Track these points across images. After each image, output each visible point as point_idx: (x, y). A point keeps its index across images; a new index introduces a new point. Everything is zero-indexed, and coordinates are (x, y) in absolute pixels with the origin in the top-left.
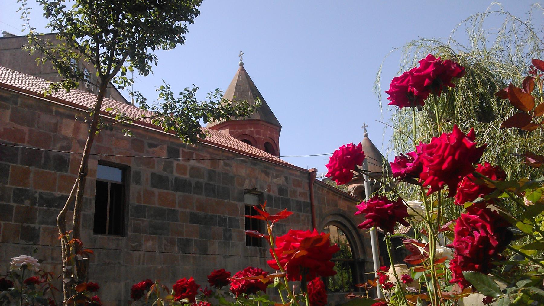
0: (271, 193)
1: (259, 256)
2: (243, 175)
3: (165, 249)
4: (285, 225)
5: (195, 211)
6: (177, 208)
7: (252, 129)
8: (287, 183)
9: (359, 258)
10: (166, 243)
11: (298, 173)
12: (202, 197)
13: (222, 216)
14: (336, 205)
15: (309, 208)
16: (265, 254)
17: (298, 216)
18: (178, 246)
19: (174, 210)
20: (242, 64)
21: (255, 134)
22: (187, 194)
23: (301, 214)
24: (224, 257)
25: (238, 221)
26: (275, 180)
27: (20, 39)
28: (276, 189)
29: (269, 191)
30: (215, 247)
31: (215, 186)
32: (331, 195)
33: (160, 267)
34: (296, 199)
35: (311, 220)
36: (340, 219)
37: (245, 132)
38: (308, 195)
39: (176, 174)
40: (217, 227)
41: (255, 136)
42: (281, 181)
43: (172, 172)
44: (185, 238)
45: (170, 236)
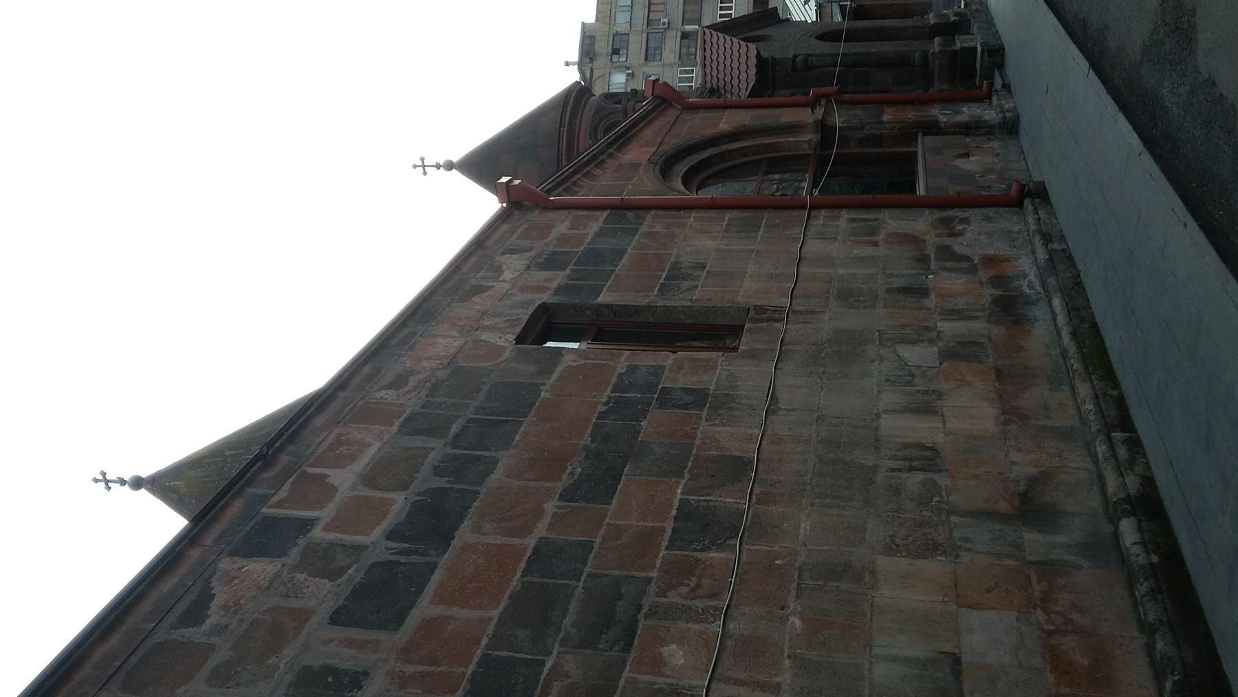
0: (554, 285)
3: (713, 596)
5: (559, 487)
6: (531, 542)
8: (529, 250)
9: (809, 142)
10: (685, 590)
11: (505, 228)
12: (506, 459)
13: (601, 408)
15: (630, 215)
18: (706, 549)
19: (536, 550)
22: (476, 504)
24: (775, 413)
25: (632, 369)
28: (540, 276)
31: (471, 420)
32: (597, 172)
33: (797, 622)
35: (674, 212)
36: (682, 168)
44: (669, 526)
45: (654, 574)
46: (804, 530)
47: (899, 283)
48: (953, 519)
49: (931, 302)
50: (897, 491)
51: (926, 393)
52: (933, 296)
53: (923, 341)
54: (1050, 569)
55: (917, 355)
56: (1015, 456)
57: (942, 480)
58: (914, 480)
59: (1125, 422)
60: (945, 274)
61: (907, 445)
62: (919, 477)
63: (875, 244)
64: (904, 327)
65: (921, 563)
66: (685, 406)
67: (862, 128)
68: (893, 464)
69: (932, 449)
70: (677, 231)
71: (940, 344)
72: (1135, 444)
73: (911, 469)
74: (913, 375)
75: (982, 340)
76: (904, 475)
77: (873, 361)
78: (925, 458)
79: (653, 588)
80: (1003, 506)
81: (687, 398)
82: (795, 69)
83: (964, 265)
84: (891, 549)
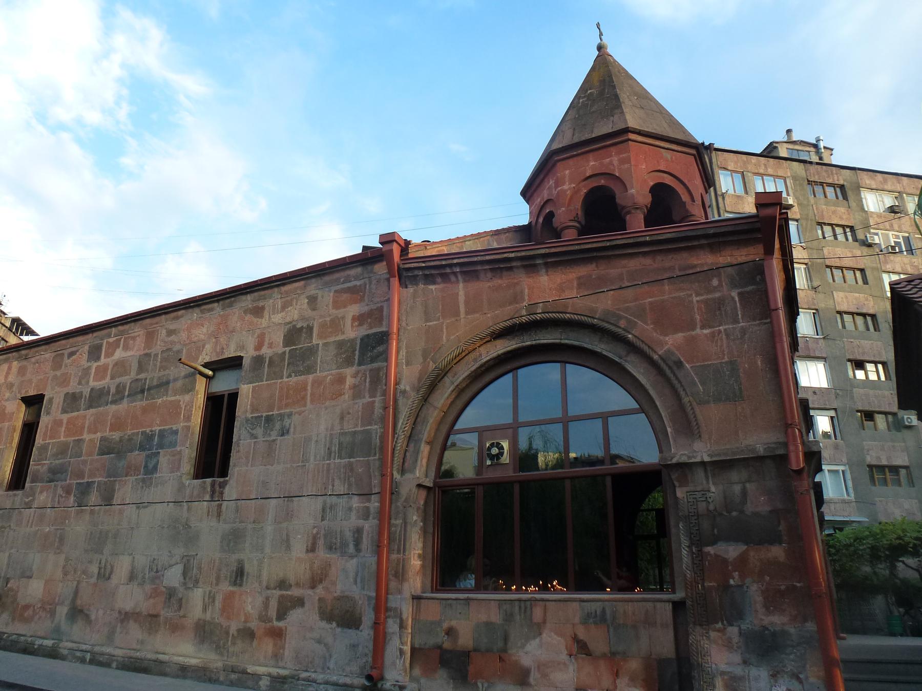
1: (207, 497)
2: (202, 337)
4: (290, 415)
5: (107, 434)
13: (148, 430)
14: (516, 299)
16: (222, 493)
18: (75, 496)
20: (600, 48)
24: (138, 508)
26: (278, 318)
29: (258, 347)
30: (126, 490)
34: (340, 337)
39: (92, 383)
40: (137, 452)
43: (88, 382)
44: (86, 480)
46: (78, 528)
47: (247, 568)
48: (75, 583)
49: (226, 587)
50: (90, 562)
51: (144, 577)
52: (231, 588)
53: (185, 578)
54: (53, 613)
55: (173, 577)
56: (101, 612)
57: (93, 580)
58: (94, 569)
59: (93, 662)
60: (259, 600)
61: (112, 567)
62: (96, 571)
63: (312, 549)
64: (200, 569)
65: (60, 569)
66: (146, 466)
68: (103, 562)
69: (109, 578)
71: (181, 589)
72: (82, 661)
73: (100, 568)
74: (157, 572)
75: (182, 613)
76: (97, 565)
77: (170, 552)
78: (105, 575)
79: (63, 483)
80: (79, 602)
81: (151, 466)
83: (272, 613)
84: (67, 560)
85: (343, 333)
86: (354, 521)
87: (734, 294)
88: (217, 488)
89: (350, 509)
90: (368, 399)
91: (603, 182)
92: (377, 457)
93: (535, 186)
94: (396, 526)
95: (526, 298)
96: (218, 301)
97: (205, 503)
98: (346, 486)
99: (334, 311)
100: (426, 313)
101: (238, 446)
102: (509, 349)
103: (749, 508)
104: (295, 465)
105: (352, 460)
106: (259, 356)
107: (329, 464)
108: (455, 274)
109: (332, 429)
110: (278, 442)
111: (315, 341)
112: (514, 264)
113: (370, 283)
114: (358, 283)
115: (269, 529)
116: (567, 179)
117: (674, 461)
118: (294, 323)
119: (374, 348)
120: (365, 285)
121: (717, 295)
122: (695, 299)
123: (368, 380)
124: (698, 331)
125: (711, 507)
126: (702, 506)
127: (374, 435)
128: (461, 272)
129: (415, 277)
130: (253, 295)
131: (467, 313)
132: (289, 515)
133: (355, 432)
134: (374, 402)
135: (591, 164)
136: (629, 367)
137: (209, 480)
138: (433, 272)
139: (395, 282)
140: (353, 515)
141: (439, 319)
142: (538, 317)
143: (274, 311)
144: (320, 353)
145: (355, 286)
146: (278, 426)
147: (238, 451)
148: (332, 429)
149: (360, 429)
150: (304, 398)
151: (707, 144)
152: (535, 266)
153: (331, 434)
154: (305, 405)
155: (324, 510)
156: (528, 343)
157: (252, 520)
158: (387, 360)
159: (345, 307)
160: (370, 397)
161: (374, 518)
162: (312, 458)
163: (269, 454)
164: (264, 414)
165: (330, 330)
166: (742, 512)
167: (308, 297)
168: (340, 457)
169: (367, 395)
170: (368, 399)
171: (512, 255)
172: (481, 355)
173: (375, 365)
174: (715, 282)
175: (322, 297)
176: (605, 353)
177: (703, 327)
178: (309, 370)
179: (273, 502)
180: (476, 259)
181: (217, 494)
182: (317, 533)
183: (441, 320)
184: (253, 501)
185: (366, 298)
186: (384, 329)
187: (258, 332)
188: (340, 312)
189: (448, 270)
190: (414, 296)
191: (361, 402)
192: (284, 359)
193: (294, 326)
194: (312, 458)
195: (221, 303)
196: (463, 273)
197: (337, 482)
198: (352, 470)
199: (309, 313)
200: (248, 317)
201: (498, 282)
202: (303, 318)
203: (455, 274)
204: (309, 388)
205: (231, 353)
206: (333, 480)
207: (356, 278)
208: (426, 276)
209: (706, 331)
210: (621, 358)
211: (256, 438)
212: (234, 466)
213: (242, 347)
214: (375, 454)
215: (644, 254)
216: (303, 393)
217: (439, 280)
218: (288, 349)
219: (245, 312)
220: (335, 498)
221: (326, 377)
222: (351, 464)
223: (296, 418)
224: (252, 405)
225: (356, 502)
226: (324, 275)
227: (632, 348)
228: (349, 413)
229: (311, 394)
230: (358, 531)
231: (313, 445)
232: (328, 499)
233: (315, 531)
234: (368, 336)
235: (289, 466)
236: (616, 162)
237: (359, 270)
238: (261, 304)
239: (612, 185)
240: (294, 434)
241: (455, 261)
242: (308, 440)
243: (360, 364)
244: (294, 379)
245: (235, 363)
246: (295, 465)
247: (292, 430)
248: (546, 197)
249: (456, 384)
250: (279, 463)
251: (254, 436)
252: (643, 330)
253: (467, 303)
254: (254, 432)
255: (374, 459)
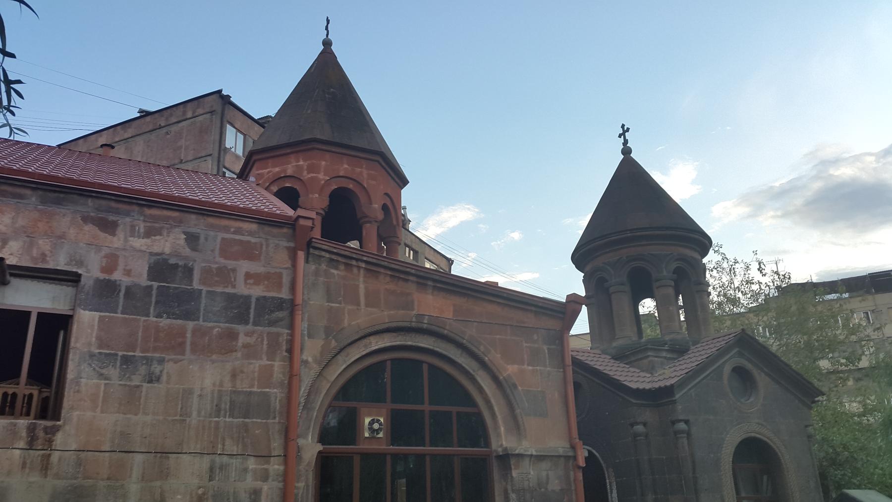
4: (161, 361)
7: (301, 163)
14: (409, 306)
16: (50, 441)
17: (232, 336)
20: (327, 43)
21: (305, 173)
23: (240, 328)
26: (138, 243)
27: (156, 115)
29: (109, 268)
34: (229, 290)
37: (285, 171)
38: (286, 280)
41: (306, 176)
42: (170, 243)
67: (513, 491)
70: (239, 354)
82: (673, 423)
85: (234, 287)
86: (250, 482)
87: (545, 348)
88: (41, 434)
89: (246, 470)
90: (265, 362)
91: (351, 186)
92: (277, 420)
93: (272, 154)
94: (298, 488)
95: (416, 307)
96: (33, 189)
97: (18, 452)
98: (240, 446)
99: (222, 261)
100: (328, 292)
101: (78, 384)
102: (394, 344)
103: (550, 487)
104: (170, 418)
105: (247, 420)
106: (109, 281)
107: (217, 423)
108: (359, 267)
109: (221, 385)
110: (144, 390)
111: (196, 285)
112: (411, 278)
113: (268, 245)
114: (253, 240)
115: (134, 487)
116: (322, 170)
117: (517, 452)
118: (166, 257)
119: (272, 312)
120: (261, 245)
121: (536, 346)
122: (525, 345)
123: (265, 342)
124: (525, 366)
125: (531, 485)
126: (526, 483)
127: (273, 399)
128: (365, 269)
129: (320, 256)
130: (98, 202)
131: (367, 305)
132: (164, 474)
133: (250, 392)
134: (272, 366)
135: (344, 168)
136: (479, 379)
137: (23, 423)
138: (340, 259)
139: (301, 255)
140: (249, 477)
141: (340, 303)
142: (425, 326)
143: (133, 232)
144: (203, 301)
145: (249, 242)
146: (143, 370)
147: (78, 391)
148: (221, 385)
149: (255, 389)
150: (182, 345)
151: (224, 93)
152: (426, 285)
153: (219, 391)
154: (183, 353)
155: (212, 469)
156: (410, 343)
157: (106, 476)
158: (292, 326)
159: (236, 259)
160: (268, 360)
161: (273, 480)
162: (195, 414)
163: (131, 400)
164: (120, 353)
165: (216, 279)
166: (546, 489)
167: (185, 233)
168: (232, 416)
169: (264, 357)
170: (265, 362)
171: (413, 271)
172: (370, 343)
173: (274, 330)
174: (535, 337)
175: (206, 239)
176: (464, 365)
177: (528, 365)
178: (189, 315)
179: (139, 458)
180: (383, 263)
181: (40, 441)
182: (204, 494)
183: (343, 305)
184: (107, 454)
185: (262, 258)
186: (285, 294)
187: (105, 251)
188: (230, 264)
189: (354, 263)
190: (317, 273)
191: (256, 365)
192: (150, 295)
193: (165, 261)
194: (195, 414)
195: (40, 193)
196: (365, 269)
197: (228, 442)
198: (247, 431)
199: (187, 251)
200: (89, 228)
201: (391, 286)
202: (177, 255)
203: (359, 267)
204: (189, 335)
205: (60, 262)
206: (224, 439)
207: (251, 233)
208: (332, 260)
209: (530, 368)
210: (474, 371)
211: (106, 379)
212: (72, 408)
213: (80, 263)
214: (275, 418)
215: (499, 303)
216: (180, 340)
217: (342, 267)
218: (155, 284)
219: (86, 219)
220: (225, 459)
221: (214, 328)
222: (246, 425)
223: (169, 367)
224: (98, 338)
225: (252, 464)
226: (208, 215)
227: (484, 365)
228: (242, 372)
229: (192, 344)
230: (255, 494)
231: (195, 400)
232: (218, 459)
233: (200, 491)
234: (265, 297)
235: (161, 418)
236: (365, 176)
237: (254, 227)
238: (112, 218)
239: (357, 191)
240: (168, 382)
241: (365, 259)
242: (189, 392)
243: (255, 324)
244: (165, 322)
245: (72, 279)
246: (170, 418)
247: (164, 378)
248: (290, 172)
249: (348, 363)
250: (146, 414)
251: (101, 376)
252: (494, 357)
253: (367, 296)
254: (104, 371)
255: (275, 423)
